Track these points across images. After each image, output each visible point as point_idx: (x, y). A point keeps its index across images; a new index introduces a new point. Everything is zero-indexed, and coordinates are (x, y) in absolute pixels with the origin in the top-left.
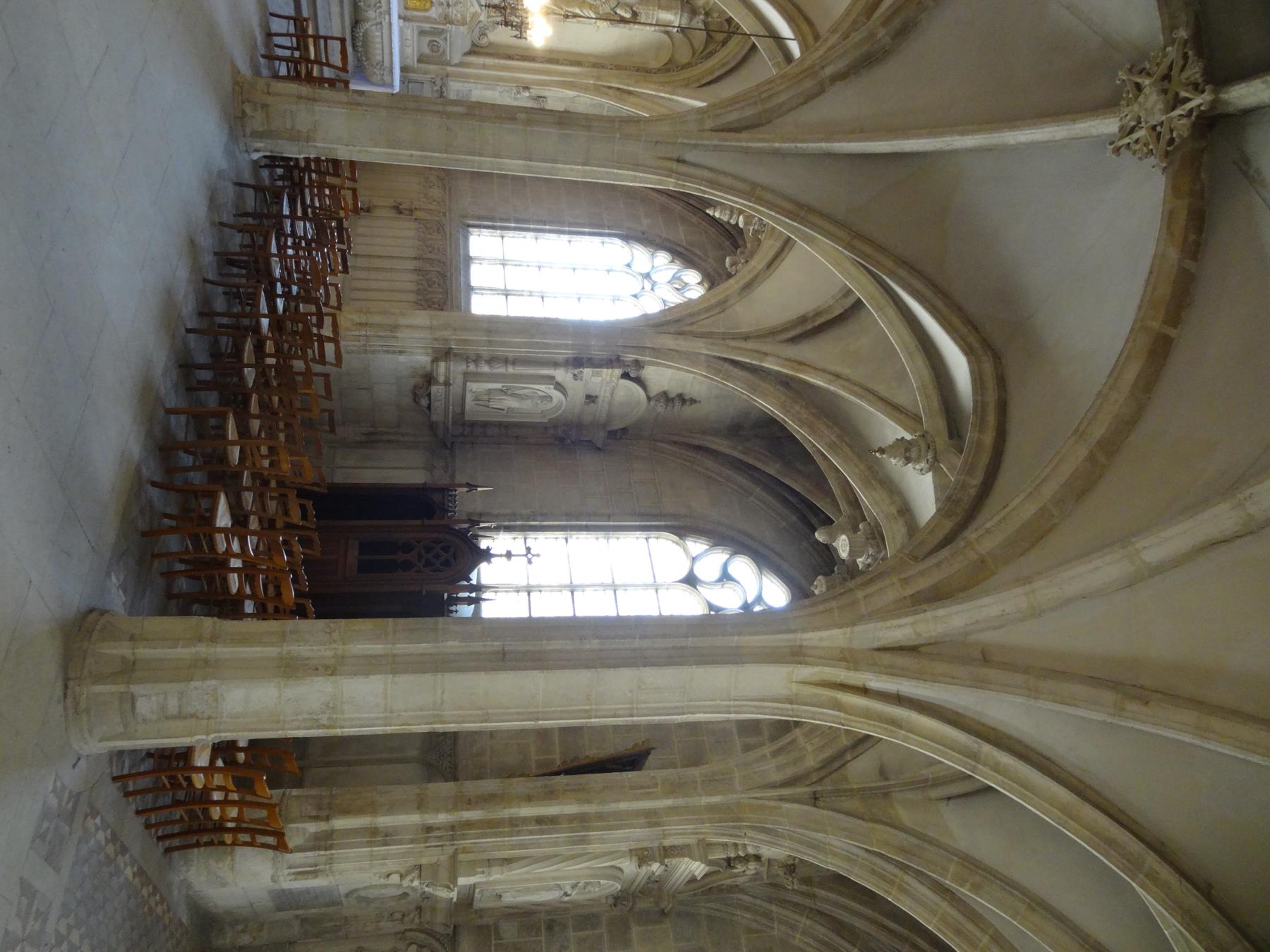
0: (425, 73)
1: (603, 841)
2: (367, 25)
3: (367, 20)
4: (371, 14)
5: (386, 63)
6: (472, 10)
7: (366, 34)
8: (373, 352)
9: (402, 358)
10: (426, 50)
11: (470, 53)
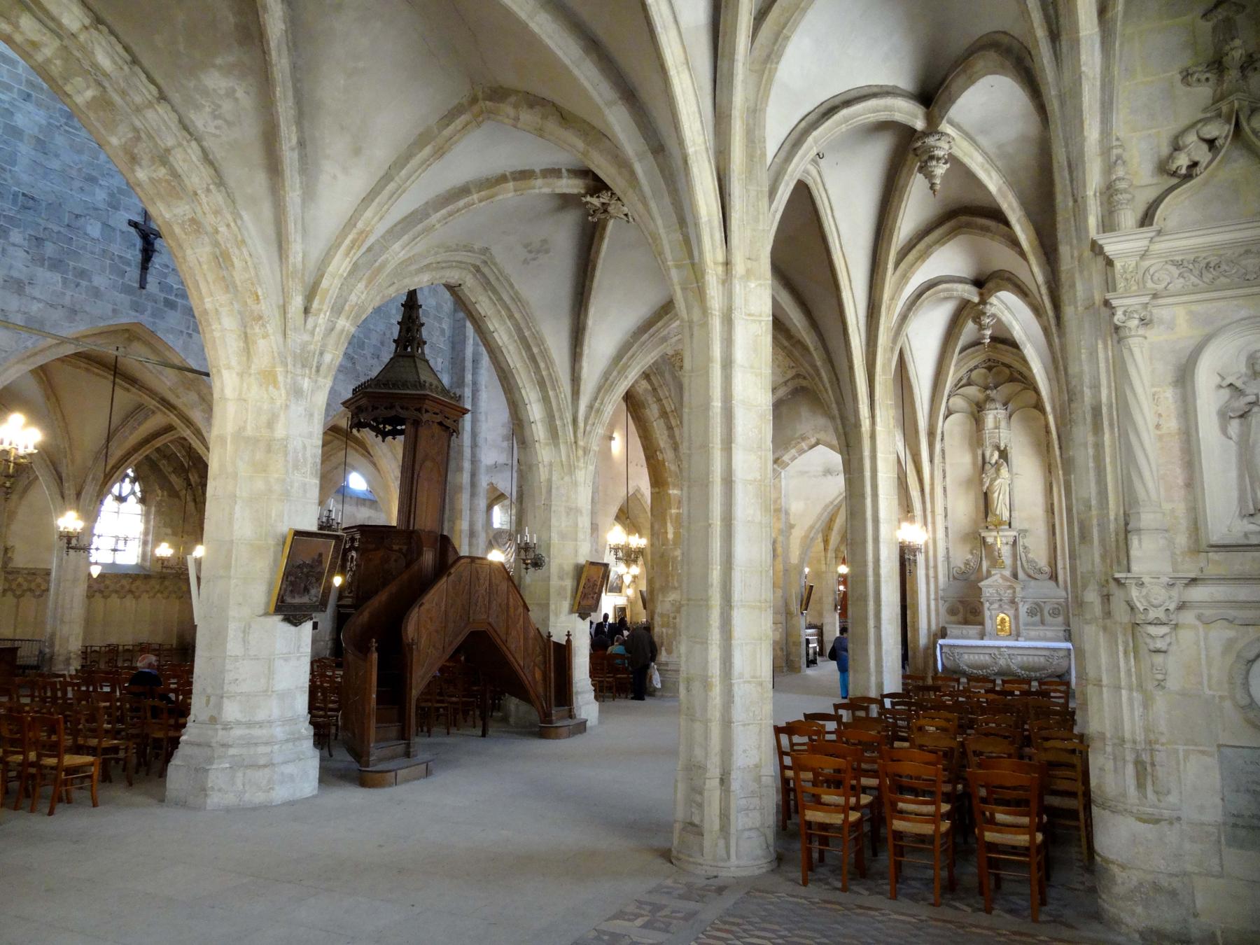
1: (1096, 387)
3: (1008, 666)
4: (1002, 662)
6: (1000, 581)
7: (1022, 668)
10: (1060, 619)
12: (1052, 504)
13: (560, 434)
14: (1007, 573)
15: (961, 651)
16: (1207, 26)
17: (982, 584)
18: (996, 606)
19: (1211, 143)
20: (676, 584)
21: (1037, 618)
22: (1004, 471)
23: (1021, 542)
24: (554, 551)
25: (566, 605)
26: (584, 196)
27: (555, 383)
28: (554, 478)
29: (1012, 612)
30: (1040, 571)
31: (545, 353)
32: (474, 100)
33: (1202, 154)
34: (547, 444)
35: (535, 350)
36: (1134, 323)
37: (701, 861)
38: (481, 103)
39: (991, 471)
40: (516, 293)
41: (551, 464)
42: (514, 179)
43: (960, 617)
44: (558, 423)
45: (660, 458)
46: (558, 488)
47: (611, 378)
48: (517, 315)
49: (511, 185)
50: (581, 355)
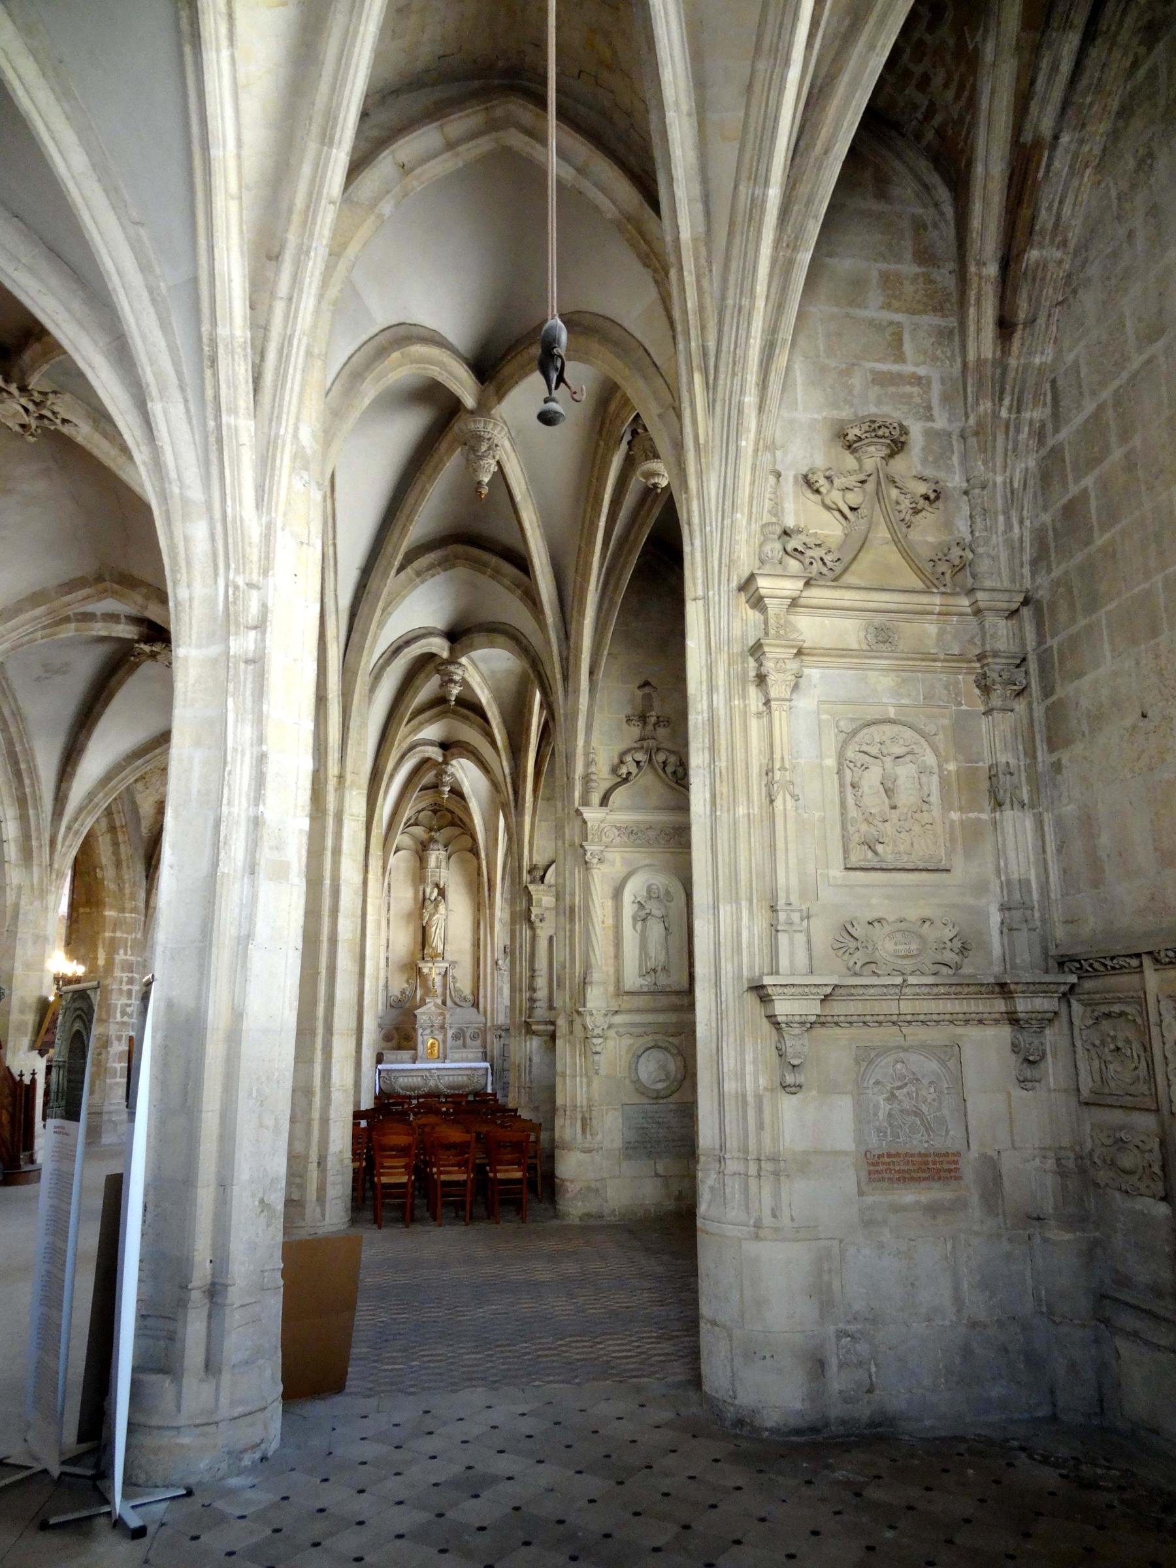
0: (492, 1043)
1: (573, 895)
2: (441, 1086)
4: (432, 1083)
5: (468, 1072)
6: (433, 1008)
8: (531, 1082)
9: (536, 1059)
10: (479, 1042)
11: (478, 1008)
12: (479, 939)
13: (35, 854)
14: (439, 1001)
15: (398, 1074)
16: (640, 693)
17: (417, 1012)
18: (428, 1031)
19: (638, 763)
20: (104, 1016)
21: (460, 1042)
22: (442, 908)
23: (451, 972)
24: (16, 982)
25: (26, 1041)
26: (138, 641)
27: (37, 800)
28: (22, 903)
29: (440, 1037)
30: (465, 1000)
31: (33, 771)
32: (100, 579)
33: (634, 770)
34: (16, 865)
35: (23, 766)
36: (595, 861)
37: (303, 1224)
38: (107, 584)
39: (430, 907)
40: (18, 708)
41: (20, 888)
42: (78, 621)
43: (394, 1042)
44: (34, 843)
45: (99, 875)
46: (26, 914)
47: (96, 800)
48: (13, 729)
49: (73, 626)
50: (72, 775)
